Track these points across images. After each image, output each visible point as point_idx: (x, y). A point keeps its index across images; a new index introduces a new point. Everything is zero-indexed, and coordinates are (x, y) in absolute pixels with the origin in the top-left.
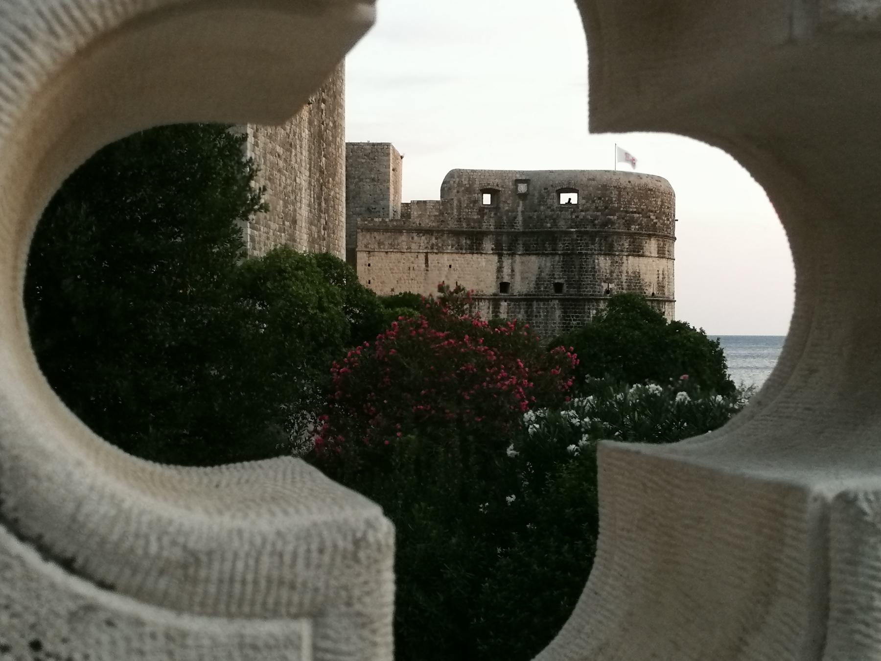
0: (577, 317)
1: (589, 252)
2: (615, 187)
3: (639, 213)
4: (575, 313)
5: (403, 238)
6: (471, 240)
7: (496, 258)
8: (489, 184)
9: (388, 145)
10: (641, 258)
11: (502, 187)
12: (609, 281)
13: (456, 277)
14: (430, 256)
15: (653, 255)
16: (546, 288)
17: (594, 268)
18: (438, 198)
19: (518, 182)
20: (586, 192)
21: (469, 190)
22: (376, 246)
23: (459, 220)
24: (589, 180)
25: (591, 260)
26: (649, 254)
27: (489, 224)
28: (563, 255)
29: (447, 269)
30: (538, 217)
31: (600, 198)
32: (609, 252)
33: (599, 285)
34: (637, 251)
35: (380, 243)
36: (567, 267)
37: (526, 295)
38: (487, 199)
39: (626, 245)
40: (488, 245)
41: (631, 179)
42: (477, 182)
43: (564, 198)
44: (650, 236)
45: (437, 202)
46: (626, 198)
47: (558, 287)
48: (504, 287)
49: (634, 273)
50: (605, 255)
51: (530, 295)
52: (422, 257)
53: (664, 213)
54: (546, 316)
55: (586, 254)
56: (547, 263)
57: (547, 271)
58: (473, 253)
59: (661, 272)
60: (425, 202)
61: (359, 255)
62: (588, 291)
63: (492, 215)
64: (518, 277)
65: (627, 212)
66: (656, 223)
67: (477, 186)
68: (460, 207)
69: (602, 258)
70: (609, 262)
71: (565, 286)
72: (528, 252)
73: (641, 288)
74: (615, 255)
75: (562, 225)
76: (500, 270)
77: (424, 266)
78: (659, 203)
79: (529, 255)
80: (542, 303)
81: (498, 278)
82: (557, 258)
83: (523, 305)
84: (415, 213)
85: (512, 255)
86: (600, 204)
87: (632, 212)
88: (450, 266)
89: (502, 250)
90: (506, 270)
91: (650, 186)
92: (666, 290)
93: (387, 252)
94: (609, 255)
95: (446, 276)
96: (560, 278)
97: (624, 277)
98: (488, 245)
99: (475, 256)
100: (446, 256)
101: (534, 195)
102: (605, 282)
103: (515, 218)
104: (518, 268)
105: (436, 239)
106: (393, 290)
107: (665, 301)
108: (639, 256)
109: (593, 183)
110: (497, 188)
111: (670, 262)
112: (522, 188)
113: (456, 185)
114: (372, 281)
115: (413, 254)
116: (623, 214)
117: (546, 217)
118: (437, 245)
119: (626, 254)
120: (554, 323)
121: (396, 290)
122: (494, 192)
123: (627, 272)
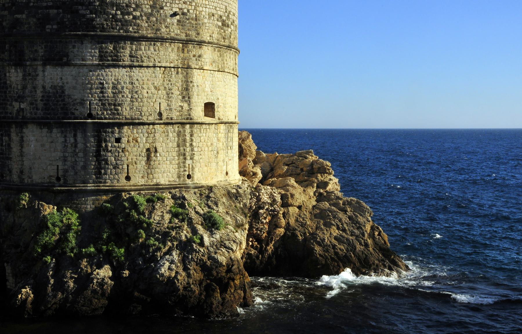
3: (58, 8)
10: (66, 69)
12: (20, 98)
17: (5, 83)
32: (19, 63)
33: (11, 105)
34: (59, 59)
39: (41, 52)
44: (81, 39)
49: (54, 87)
70: (20, 75)
74: (26, 66)
87: (47, 7)
97: (39, 93)
102: (16, 101)
107: (120, 125)
123: (44, 87)
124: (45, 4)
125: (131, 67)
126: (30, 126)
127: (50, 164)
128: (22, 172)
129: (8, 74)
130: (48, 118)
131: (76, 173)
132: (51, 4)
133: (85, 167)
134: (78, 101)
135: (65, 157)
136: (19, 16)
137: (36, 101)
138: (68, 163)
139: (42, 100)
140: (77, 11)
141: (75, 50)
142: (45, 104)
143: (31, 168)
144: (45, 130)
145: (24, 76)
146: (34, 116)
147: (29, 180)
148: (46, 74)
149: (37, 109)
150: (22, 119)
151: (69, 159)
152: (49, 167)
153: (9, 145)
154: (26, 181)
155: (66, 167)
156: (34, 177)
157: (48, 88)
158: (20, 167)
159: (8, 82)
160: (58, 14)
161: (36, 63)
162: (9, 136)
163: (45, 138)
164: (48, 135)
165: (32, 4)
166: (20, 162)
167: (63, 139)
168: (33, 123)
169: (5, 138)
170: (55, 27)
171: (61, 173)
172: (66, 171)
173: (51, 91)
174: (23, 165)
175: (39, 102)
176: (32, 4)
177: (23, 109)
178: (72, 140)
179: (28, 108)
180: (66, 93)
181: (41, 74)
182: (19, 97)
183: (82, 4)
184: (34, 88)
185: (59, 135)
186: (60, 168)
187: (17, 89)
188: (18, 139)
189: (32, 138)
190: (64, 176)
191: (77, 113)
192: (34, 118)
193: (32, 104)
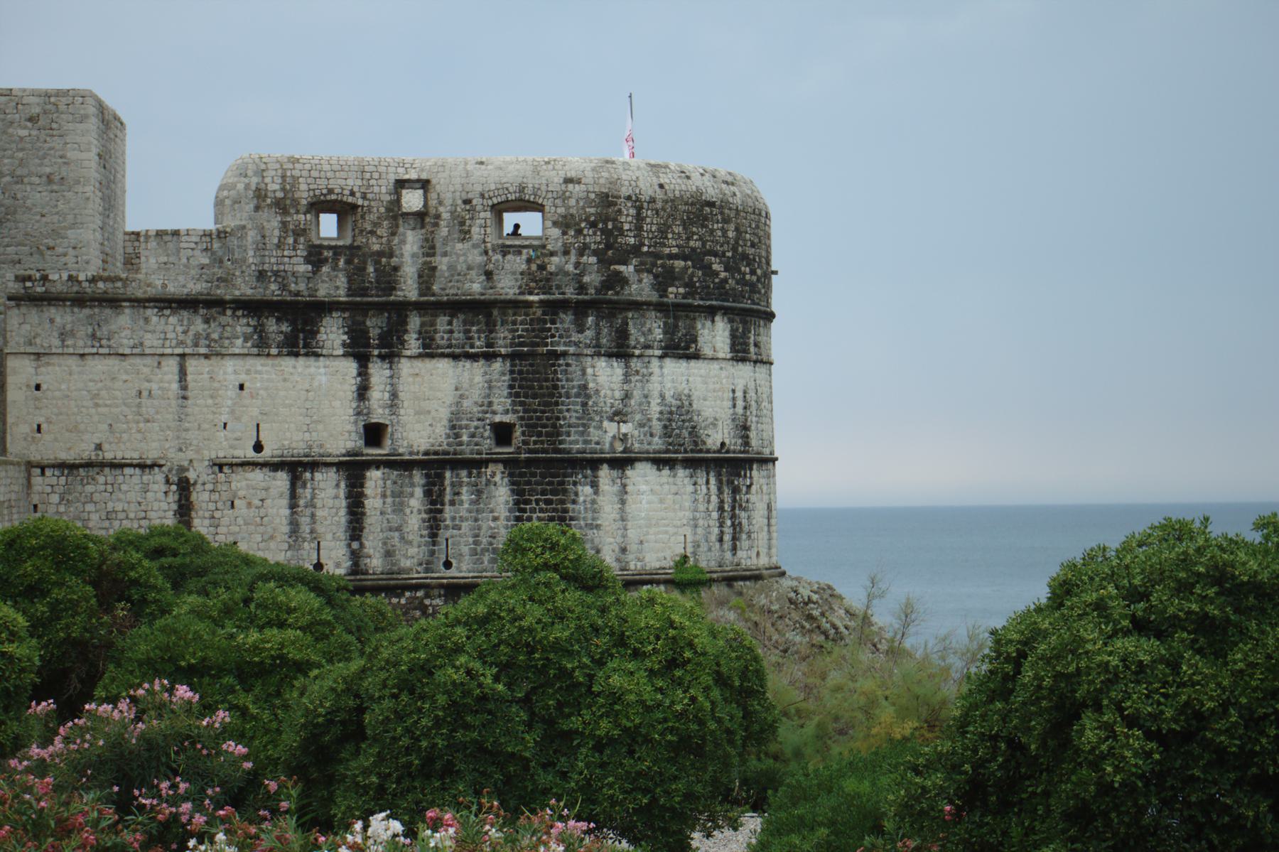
0: (548, 502)
1: (572, 350)
2: (629, 198)
3: (685, 258)
4: (543, 493)
5: (123, 324)
6: (289, 323)
7: (350, 367)
8: (331, 191)
9: (84, 95)
10: (693, 363)
11: (364, 197)
12: (619, 416)
13: (255, 412)
14: (191, 365)
15: (721, 355)
16: (473, 436)
17: (585, 387)
18: (207, 222)
19: (401, 184)
20: (561, 210)
21: (282, 206)
22: (57, 342)
23: (261, 275)
24: (568, 181)
25: (575, 369)
26: (707, 351)
27: (333, 285)
28: (512, 357)
29: (232, 392)
30: (451, 267)
31: (593, 225)
32: (621, 351)
33: (600, 427)
34: (682, 347)
35: (63, 336)
36: (521, 388)
37: (426, 453)
38: (328, 225)
39: (658, 334)
40: (333, 333)
41: (664, 179)
42: (303, 187)
43: (510, 219)
44: (711, 312)
45: (207, 234)
46: (651, 224)
47: (502, 433)
48: (374, 434)
49: (678, 397)
50: (609, 355)
51: (436, 453)
52: (171, 366)
53: (745, 257)
54: (476, 502)
55: (564, 354)
56: (473, 376)
57: (476, 394)
58: (297, 355)
59: (739, 394)
60: (176, 233)
61: (11, 363)
62: (574, 443)
63: (341, 263)
64: (407, 411)
65: (657, 256)
66: (725, 281)
67: (304, 196)
68: (261, 247)
69: (602, 363)
71: (518, 433)
72: (430, 351)
73: (693, 431)
74: (633, 355)
75: (507, 287)
76: (363, 392)
77: (175, 386)
78: (731, 234)
79: (432, 356)
80: (464, 473)
81: (358, 414)
82: (497, 365)
83: (418, 477)
84: (151, 260)
85: (391, 356)
86: (594, 239)
87: (672, 257)
88: (241, 387)
89: (368, 345)
90: (378, 395)
91: (711, 193)
92: (753, 434)
93: (82, 355)
94: (618, 356)
95: (232, 412)
96: (507, 412)
97: (655, 408)
98: (333, 333)
99: (302, 360)
100: (230, 365)
101: (438, 216)
102: (611, 420)
103: (396, 269)
104: (408, 387)
105: (207, 321)
106: (99, 447)
108: (689, 357)
109: (576, 189)
110: (350, 199)
111: (762, 369)
112: (412, 200)
113: (251, 194)
114: (44, 427)
115: (148, 360)
116: (649, 260)
117: (469, 268)
118: (207, 337)
119: (658, 352)
120: (495, 519)
121: (106, 446)
122: (344, 210)
123: (662, 397)
124: (667, 251)
125: (755, 362)
126: (639, 465)
127: (675, 534)
128: (624, 550)
129: (589, 371)
130: (667, 451)
131: (710, 550)
132: (675, 250)
133: (721, 540)
134: (710, 420)
135: (694, 519)
136: (622, 268)
137: (649, 420)
138: (700, 531)
139: (659, 420)
140: (709, 266)
141: (706, 332)
142: (665, 427)
143: (641, 542)
144: (666, 472)
145: (626, 375)
146: (646, 447)
147: (639, 564)
148: (665, 371)
149: (652, 435)
150: (624, 452)
151: (701, 522)
152: (673, 539)
153: (594, 502)
154: (632, 567)
155: (698, 537)
156: (647, 559)
157: (668, 394)
158: (619, 540)
159: (591, 385)
160: (686, 268)
161: (650, 352)
162: (594, 485)
163: (666, 487)
164: (671, 480)
165: (645, 249)
166: (620, 532)
167: (690, 488)
168: (647, 459)
169: (588, 490)
170: (681, 290)
171: (689, 550)
172: (697, 545)
173: (674, 402)
174: (624, 536)
175: (655, 422)
176: (645, 249)
177: (625, 435)
178: (704, 487)
179: (636, 433)
180: (695, 406)
181: (656, 370)
182: (617, 413)
183: (715, 254)
184: (646, 396)
185: (687, 480)
186: (689, 539)
187: (613, 397)
188: (616, 488)
189: (643, 488)
190: (694, 553)
191: (709, 441)
192: (648, 452)
193: (641, 425)
